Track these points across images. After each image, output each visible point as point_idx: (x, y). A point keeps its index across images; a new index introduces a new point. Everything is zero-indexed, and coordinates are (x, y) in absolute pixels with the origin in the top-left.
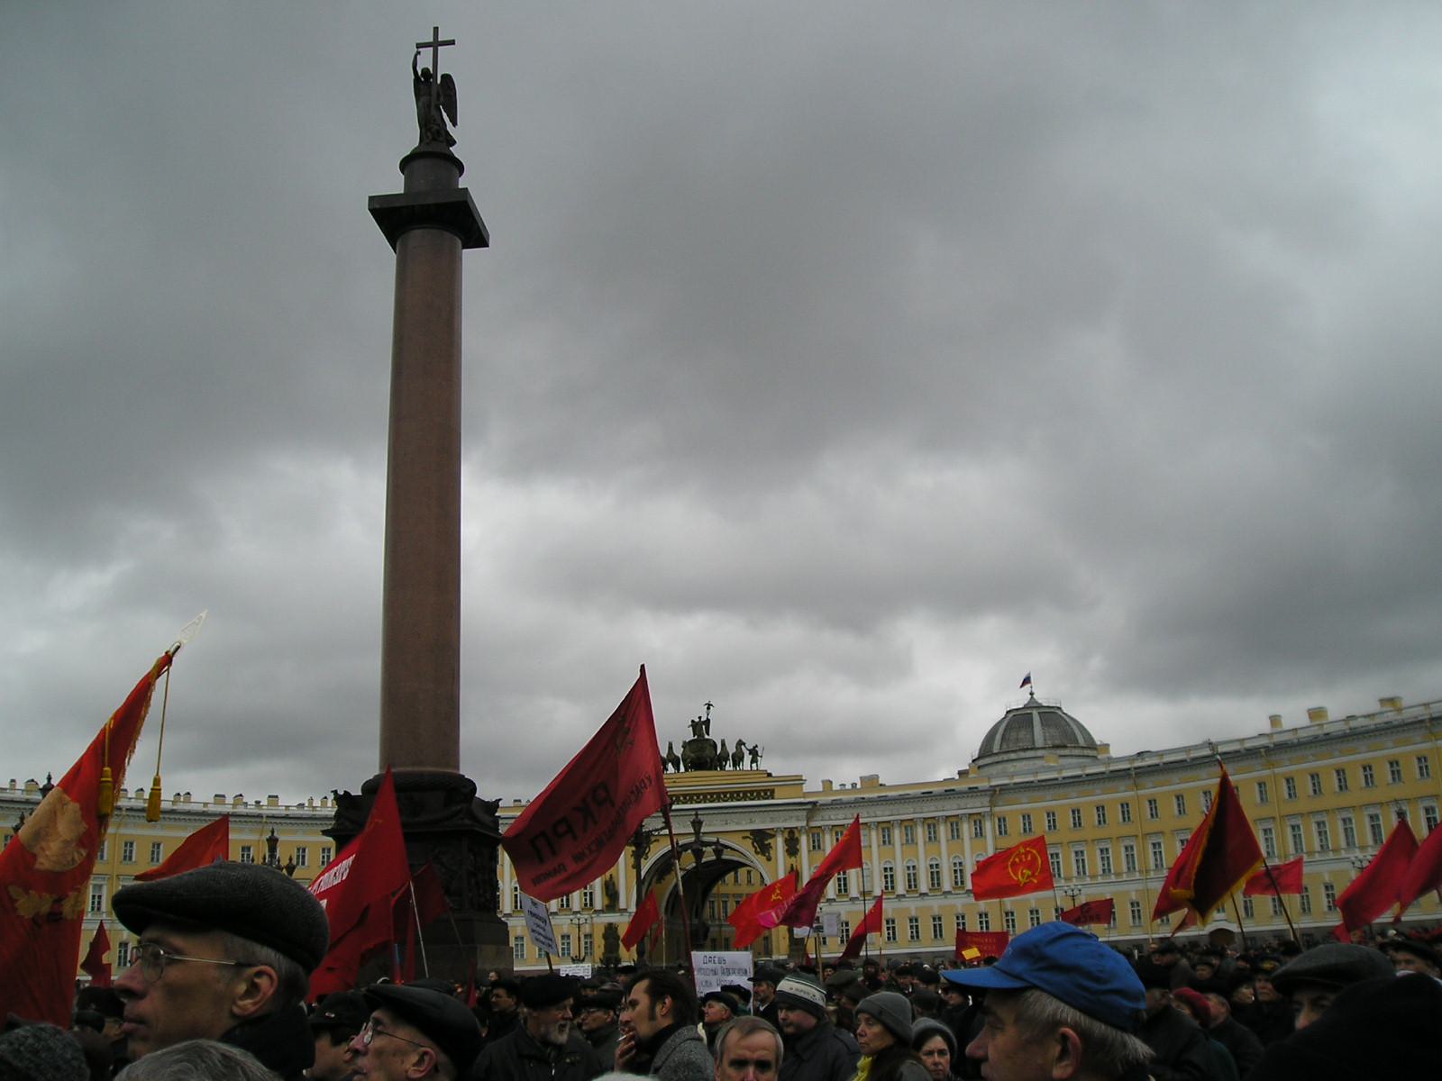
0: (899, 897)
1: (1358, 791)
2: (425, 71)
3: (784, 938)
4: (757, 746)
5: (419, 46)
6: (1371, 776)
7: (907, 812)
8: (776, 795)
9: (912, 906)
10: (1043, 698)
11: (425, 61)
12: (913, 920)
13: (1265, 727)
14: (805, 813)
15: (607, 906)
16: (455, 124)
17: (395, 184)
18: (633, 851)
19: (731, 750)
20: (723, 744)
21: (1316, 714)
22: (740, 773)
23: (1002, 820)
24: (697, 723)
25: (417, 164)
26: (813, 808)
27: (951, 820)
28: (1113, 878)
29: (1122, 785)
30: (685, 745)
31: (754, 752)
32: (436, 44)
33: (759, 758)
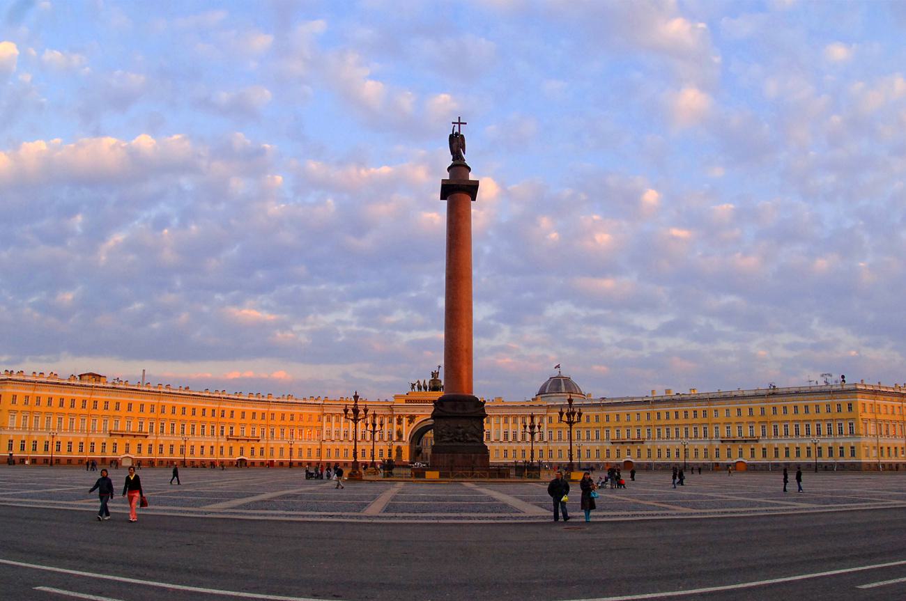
2: (457, 134)
5: (453, 123)
7: (515, 412)
10: (564, 374)
11: (456, 130)
23: (550, 418)
25: (453, 168)
29: (596, 409)
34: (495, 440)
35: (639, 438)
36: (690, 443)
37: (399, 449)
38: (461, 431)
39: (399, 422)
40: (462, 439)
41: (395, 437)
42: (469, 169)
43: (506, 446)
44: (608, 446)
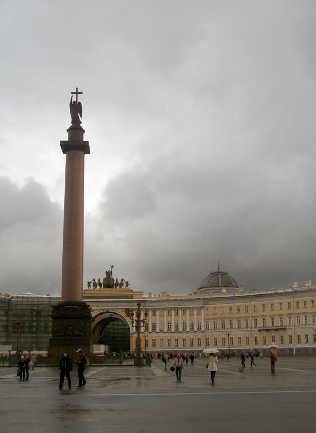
5: (72, 93)
7: (177, 305)
10: (222, 270)
11: (74, 99)
16: (81, 117)
17: (66, 138)
19: (119, 282)
28: (241, 330)
30: (104, 279)
31: (127, 283)
32: (77, 93)
34: (160, 331)
36: (232, 333)
38: (70, 328)
40: (71, 334)
42: (84, 131)
43: (169, 335)
44: (256, 334)
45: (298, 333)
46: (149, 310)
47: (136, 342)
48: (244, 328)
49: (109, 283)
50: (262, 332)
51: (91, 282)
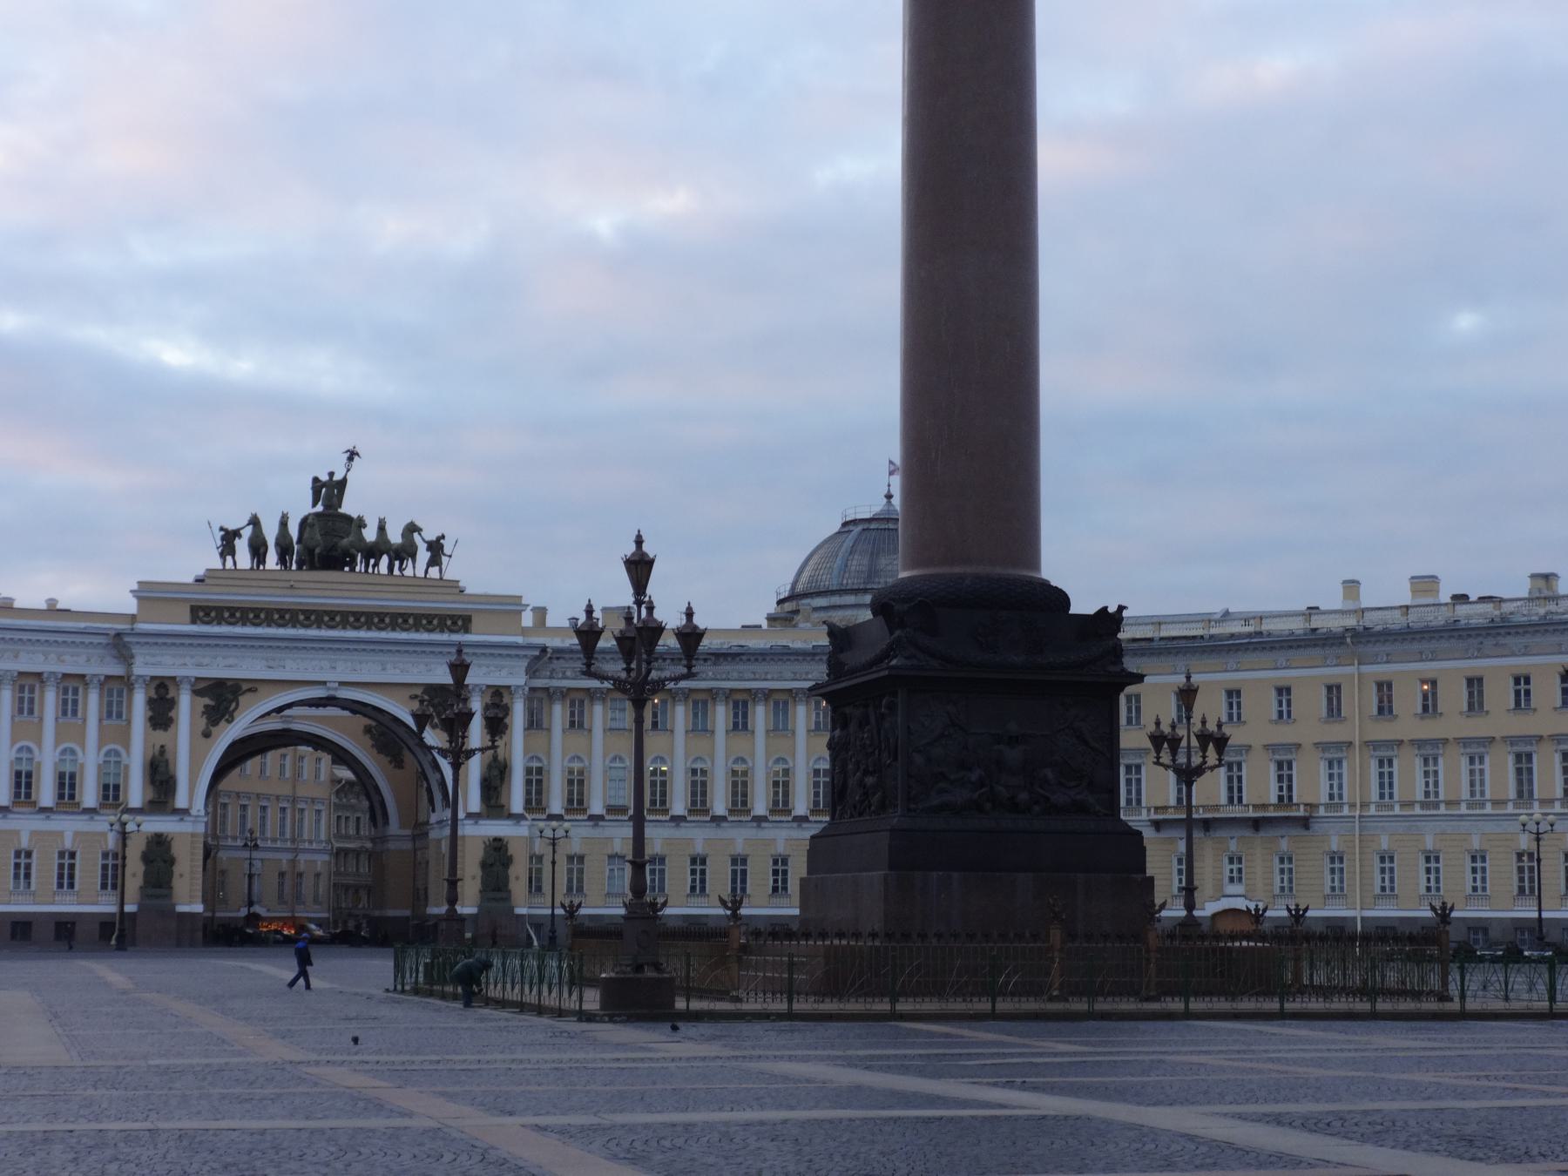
0: (678, 820)
1: (1500, 719)
3: (474, 878)
4: (443, 537)
6: (1528, 693)
8: (475, 624)
9: (698, 837)
12: (698, 861)
13: (1332, 599)
14: (525, 663)
15: (151, 802)
18: (206, 706)
19: (395, 536)
20: (382, 528)
21: (1425, 584)
22: (402, 581)
24: (324, 485)
26: (541, 658)
27: (776, 696)
30: (304, 523)
31: (436, 548)
33: (444, 559)
34: (611, 809)
35: (1285, 800)
37: (159, 850)
39: (161, 715)
40: (1023, 796)
41: (136, 793)
45: (1385, 843)
46: (592, 699)
47: (485, 865)
48: (1411, 804)
49: (329, 538)
50: (1165, 834)
51: (236, 533)
